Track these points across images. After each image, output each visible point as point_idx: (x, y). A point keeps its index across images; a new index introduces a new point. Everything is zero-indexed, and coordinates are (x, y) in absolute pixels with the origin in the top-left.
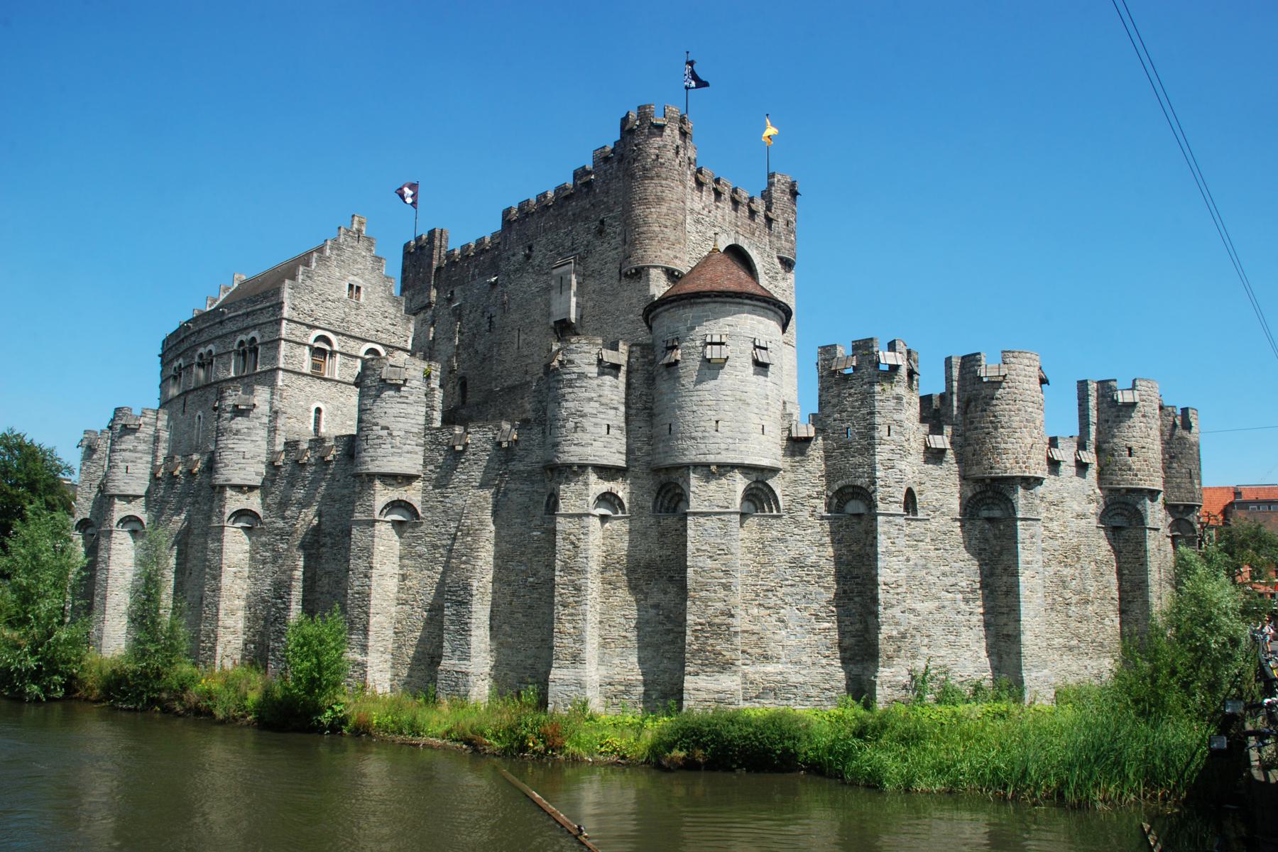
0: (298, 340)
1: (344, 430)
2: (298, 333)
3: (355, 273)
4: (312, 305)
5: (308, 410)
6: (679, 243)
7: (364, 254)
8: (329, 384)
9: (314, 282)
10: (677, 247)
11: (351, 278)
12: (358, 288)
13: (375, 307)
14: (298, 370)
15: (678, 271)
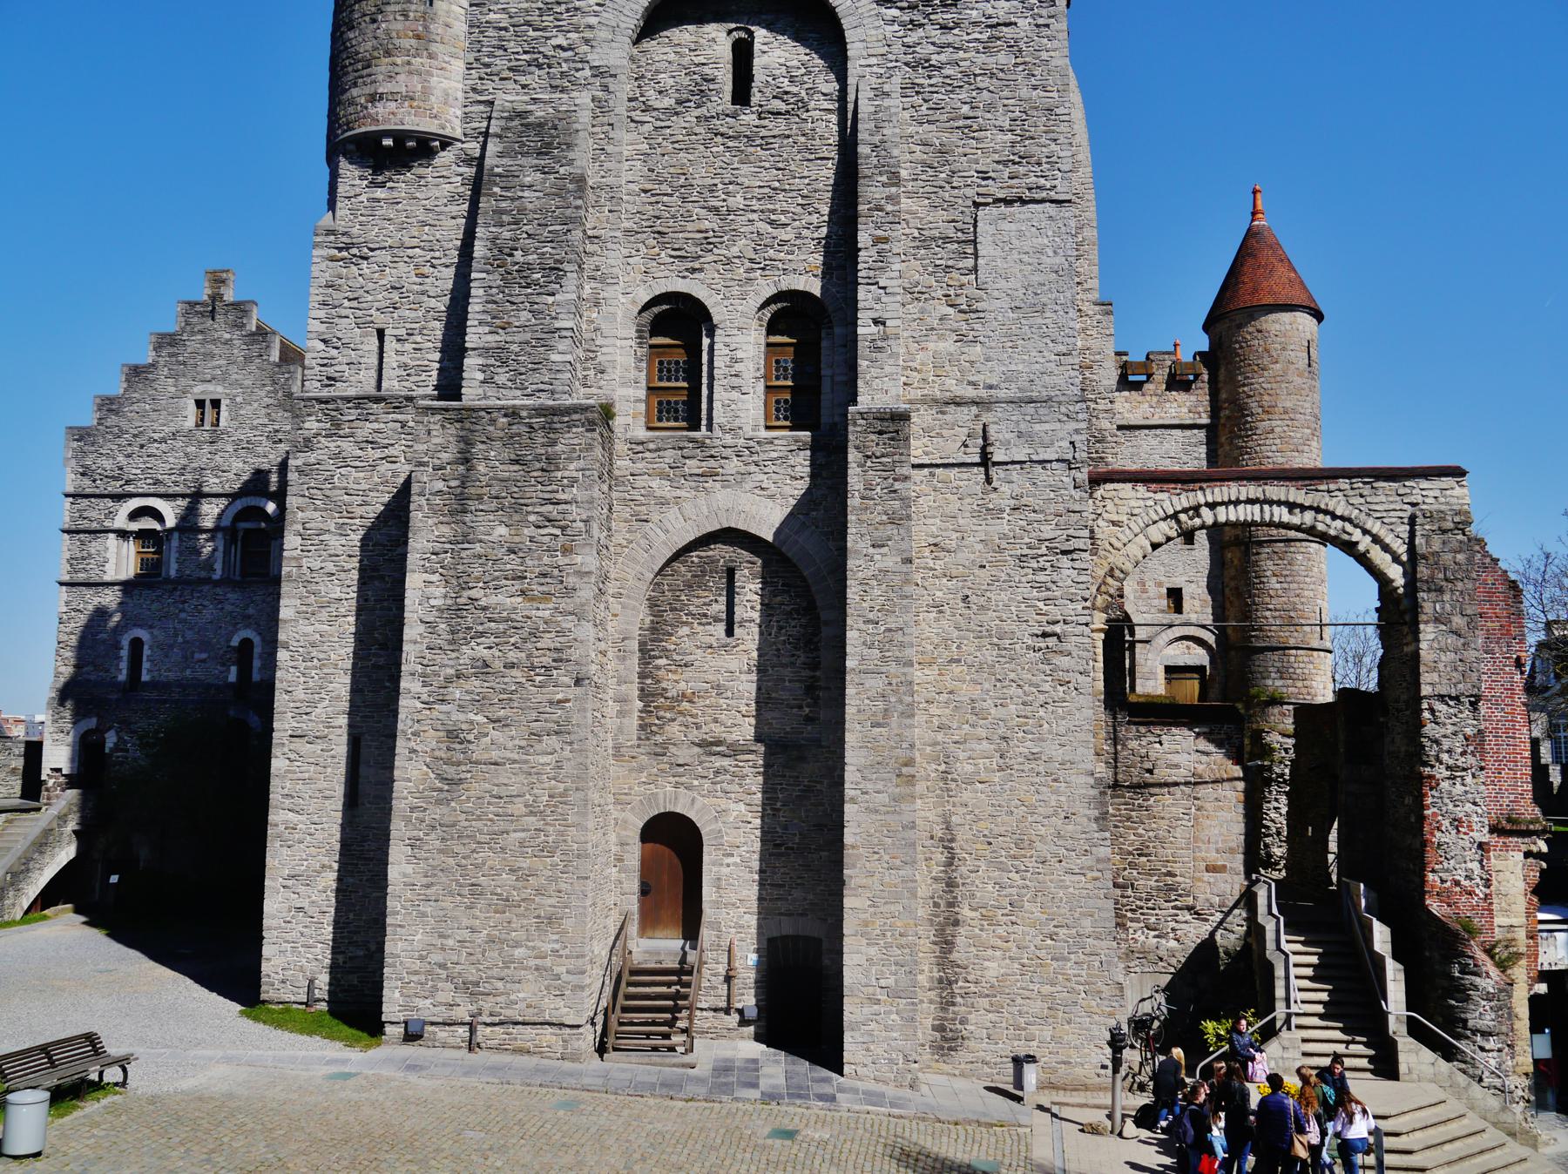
0: (95, 526)
1: (188, 672)
2: (93, 514)
3: (209, 377)
4: (121, 458)
5: (118, 647)
6: (388, 53)
7: (227, 336)
8: (159, 592)
9: (124, 416)
10: (382, 67)
11: (200, 390)
12: (216, 404)
13: (255, 428)
14: (97, 579)
15: (387, 133)
